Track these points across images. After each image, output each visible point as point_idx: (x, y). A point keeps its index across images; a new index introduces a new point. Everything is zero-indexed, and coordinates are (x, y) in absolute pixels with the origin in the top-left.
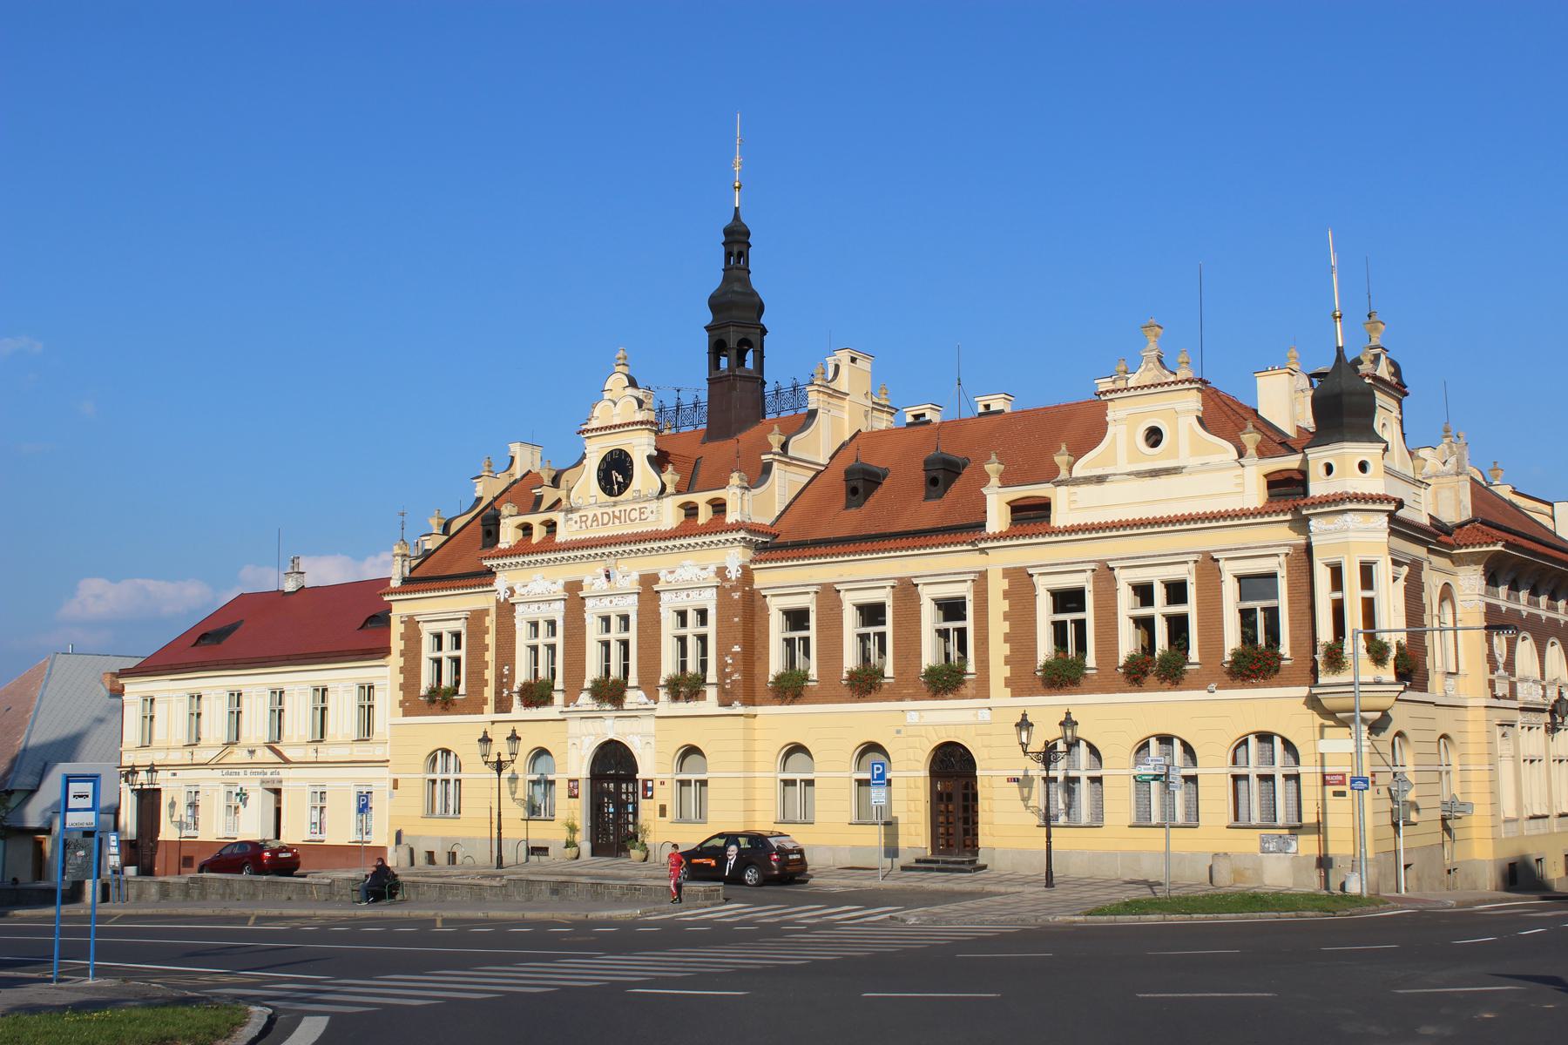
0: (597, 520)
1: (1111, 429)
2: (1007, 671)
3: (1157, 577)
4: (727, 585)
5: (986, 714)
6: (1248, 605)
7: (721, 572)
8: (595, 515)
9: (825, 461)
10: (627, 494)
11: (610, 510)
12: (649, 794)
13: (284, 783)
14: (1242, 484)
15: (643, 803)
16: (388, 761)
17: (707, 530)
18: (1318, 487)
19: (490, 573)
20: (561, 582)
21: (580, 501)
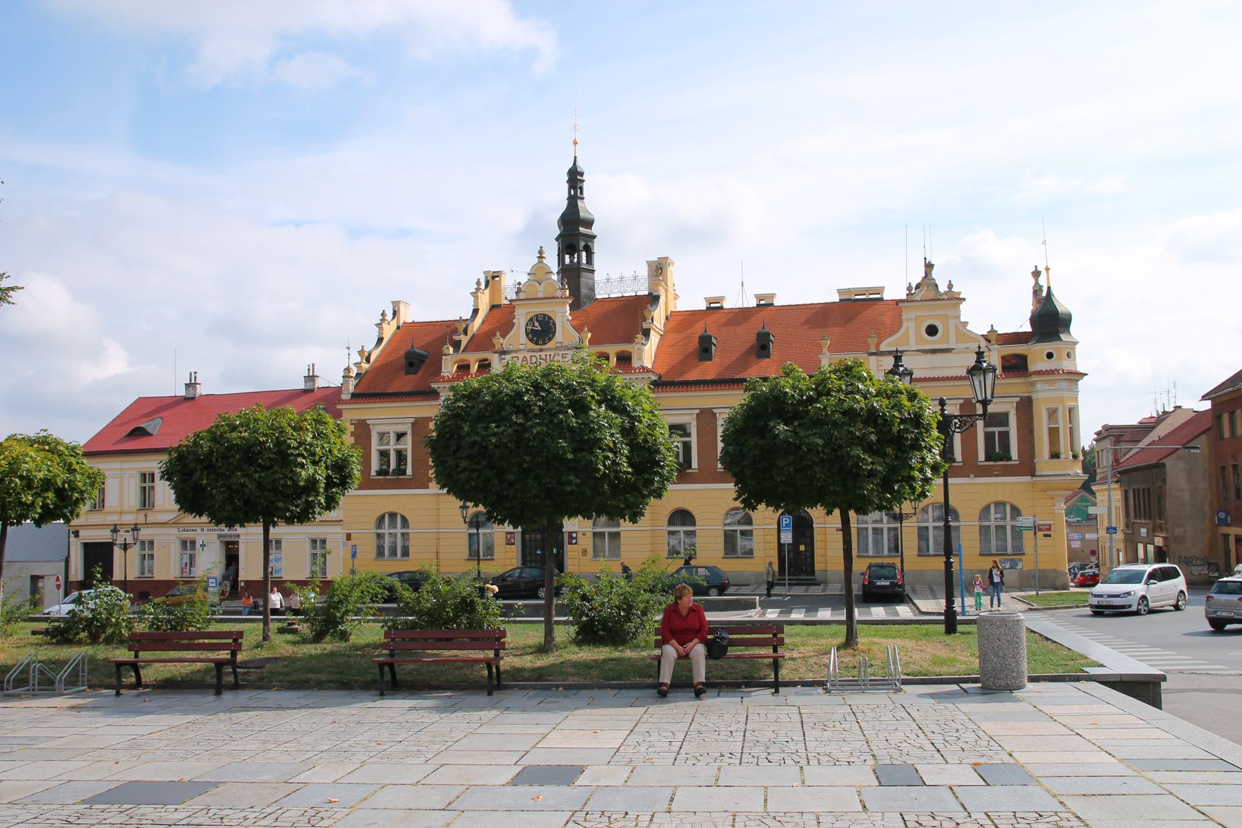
0: (526, 360)
1: (905, 325)
6: (991, 429)
8: (525, 357)
11: (537, 354)
12: (574, 541)
13: (241, 537)
16: (341, 521)
21: (511, 347)
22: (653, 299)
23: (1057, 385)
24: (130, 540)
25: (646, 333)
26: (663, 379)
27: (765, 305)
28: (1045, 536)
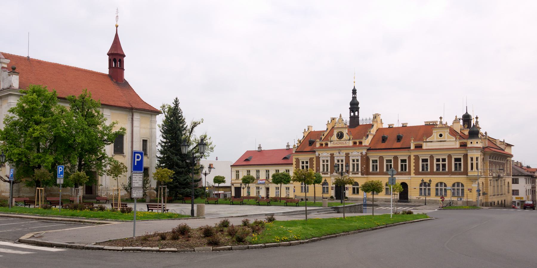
1: (433, 134)
2: (414, 171)
3: (441, 158)
4: (363, 155)
5: (410, 178)
7: (361, 153)
9: (375, 134)
10: (343, 139)
11: (339, 142)
13: (270, 186)
14: (456, 144)
15: (346, 191)
17: (358, 146)
18: (469, 145)
19: (314, 152)
20: (329, 154)
22: (372, 126)
23: (473, 151)
24: (244, 187)
25: (368, 136)
26: (371, 148)
27: (404, 126)
28: (470, 192)
